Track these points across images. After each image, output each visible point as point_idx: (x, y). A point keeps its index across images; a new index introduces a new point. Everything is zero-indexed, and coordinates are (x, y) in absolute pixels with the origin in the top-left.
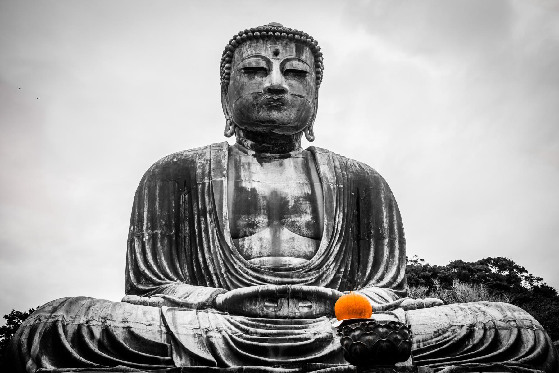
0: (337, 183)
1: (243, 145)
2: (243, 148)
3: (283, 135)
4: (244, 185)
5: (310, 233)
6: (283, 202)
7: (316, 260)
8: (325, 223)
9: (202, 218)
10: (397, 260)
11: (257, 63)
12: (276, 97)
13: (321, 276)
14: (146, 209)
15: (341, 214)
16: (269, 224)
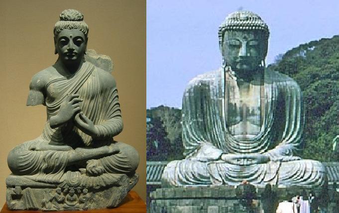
6: (248, 110)
11: (235, 43)
16: (241, 120)
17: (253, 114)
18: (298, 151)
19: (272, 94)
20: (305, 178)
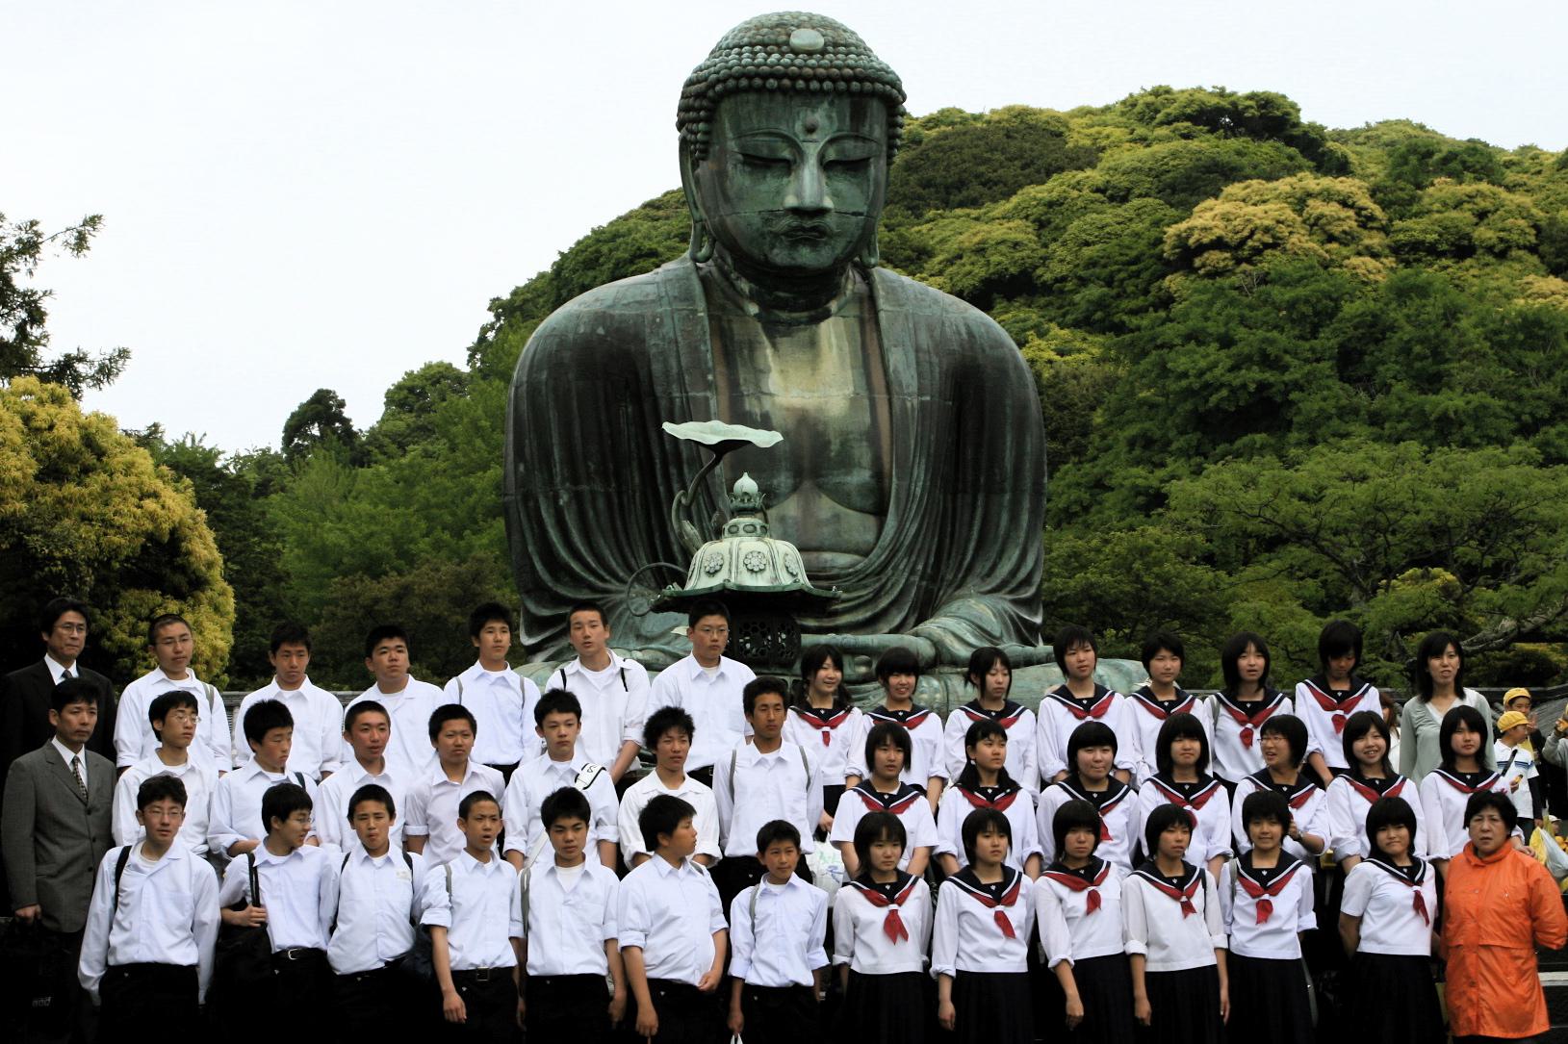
0: (921, 394)
1: (732, 285)
2: (730, 291)
4: (747, 407)
5: (869, 503)
7: (877, 557)
9: (673, 471)
10: (1022, 534)
11: (772, 150)
12: (808, 224)
14: (555, 440)
17: (846, 462)
19: (920, 375)
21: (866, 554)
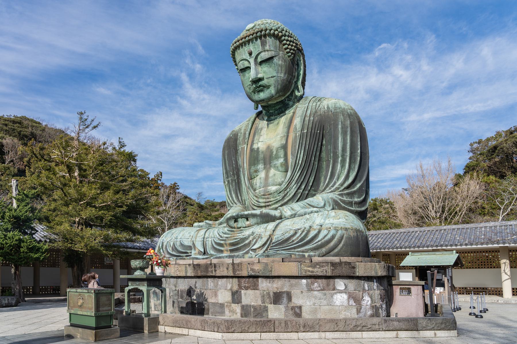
3: (277, 103)
5: (283, 169)
8: (291, 160)
10: (346, 171)
13: (285, 195)
15: (302, 152)
16: (265, 168)
17: (277, 157)
18: (350, 204)
20: (305, 241)
21: (280, 185)
